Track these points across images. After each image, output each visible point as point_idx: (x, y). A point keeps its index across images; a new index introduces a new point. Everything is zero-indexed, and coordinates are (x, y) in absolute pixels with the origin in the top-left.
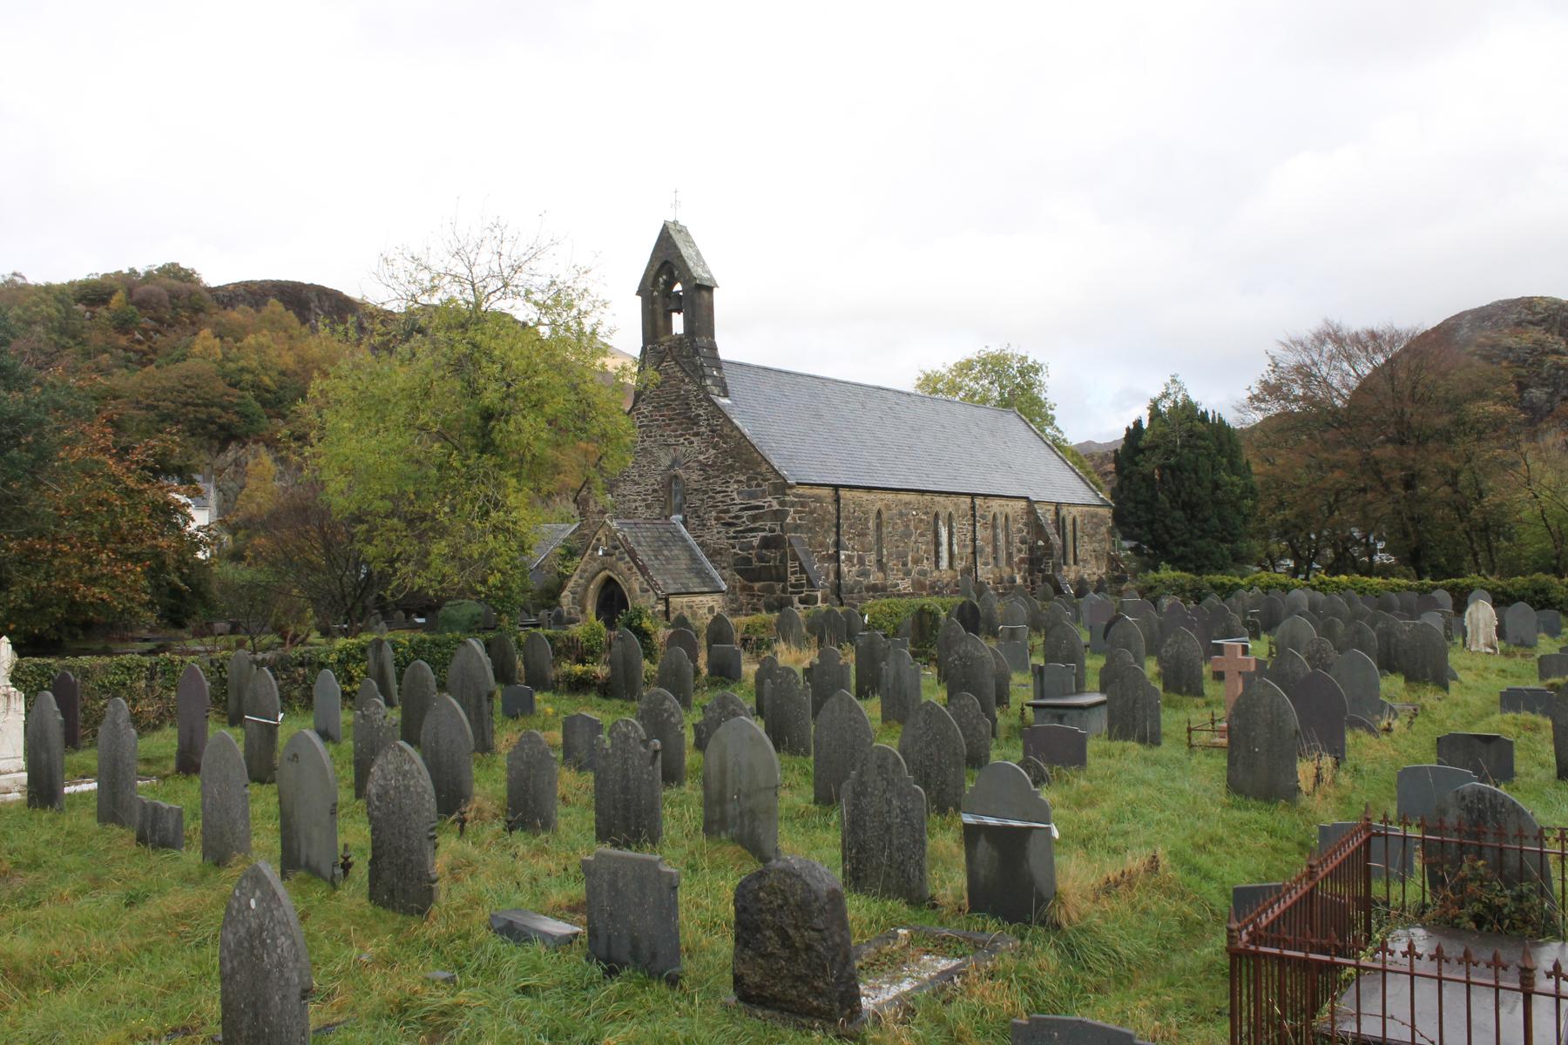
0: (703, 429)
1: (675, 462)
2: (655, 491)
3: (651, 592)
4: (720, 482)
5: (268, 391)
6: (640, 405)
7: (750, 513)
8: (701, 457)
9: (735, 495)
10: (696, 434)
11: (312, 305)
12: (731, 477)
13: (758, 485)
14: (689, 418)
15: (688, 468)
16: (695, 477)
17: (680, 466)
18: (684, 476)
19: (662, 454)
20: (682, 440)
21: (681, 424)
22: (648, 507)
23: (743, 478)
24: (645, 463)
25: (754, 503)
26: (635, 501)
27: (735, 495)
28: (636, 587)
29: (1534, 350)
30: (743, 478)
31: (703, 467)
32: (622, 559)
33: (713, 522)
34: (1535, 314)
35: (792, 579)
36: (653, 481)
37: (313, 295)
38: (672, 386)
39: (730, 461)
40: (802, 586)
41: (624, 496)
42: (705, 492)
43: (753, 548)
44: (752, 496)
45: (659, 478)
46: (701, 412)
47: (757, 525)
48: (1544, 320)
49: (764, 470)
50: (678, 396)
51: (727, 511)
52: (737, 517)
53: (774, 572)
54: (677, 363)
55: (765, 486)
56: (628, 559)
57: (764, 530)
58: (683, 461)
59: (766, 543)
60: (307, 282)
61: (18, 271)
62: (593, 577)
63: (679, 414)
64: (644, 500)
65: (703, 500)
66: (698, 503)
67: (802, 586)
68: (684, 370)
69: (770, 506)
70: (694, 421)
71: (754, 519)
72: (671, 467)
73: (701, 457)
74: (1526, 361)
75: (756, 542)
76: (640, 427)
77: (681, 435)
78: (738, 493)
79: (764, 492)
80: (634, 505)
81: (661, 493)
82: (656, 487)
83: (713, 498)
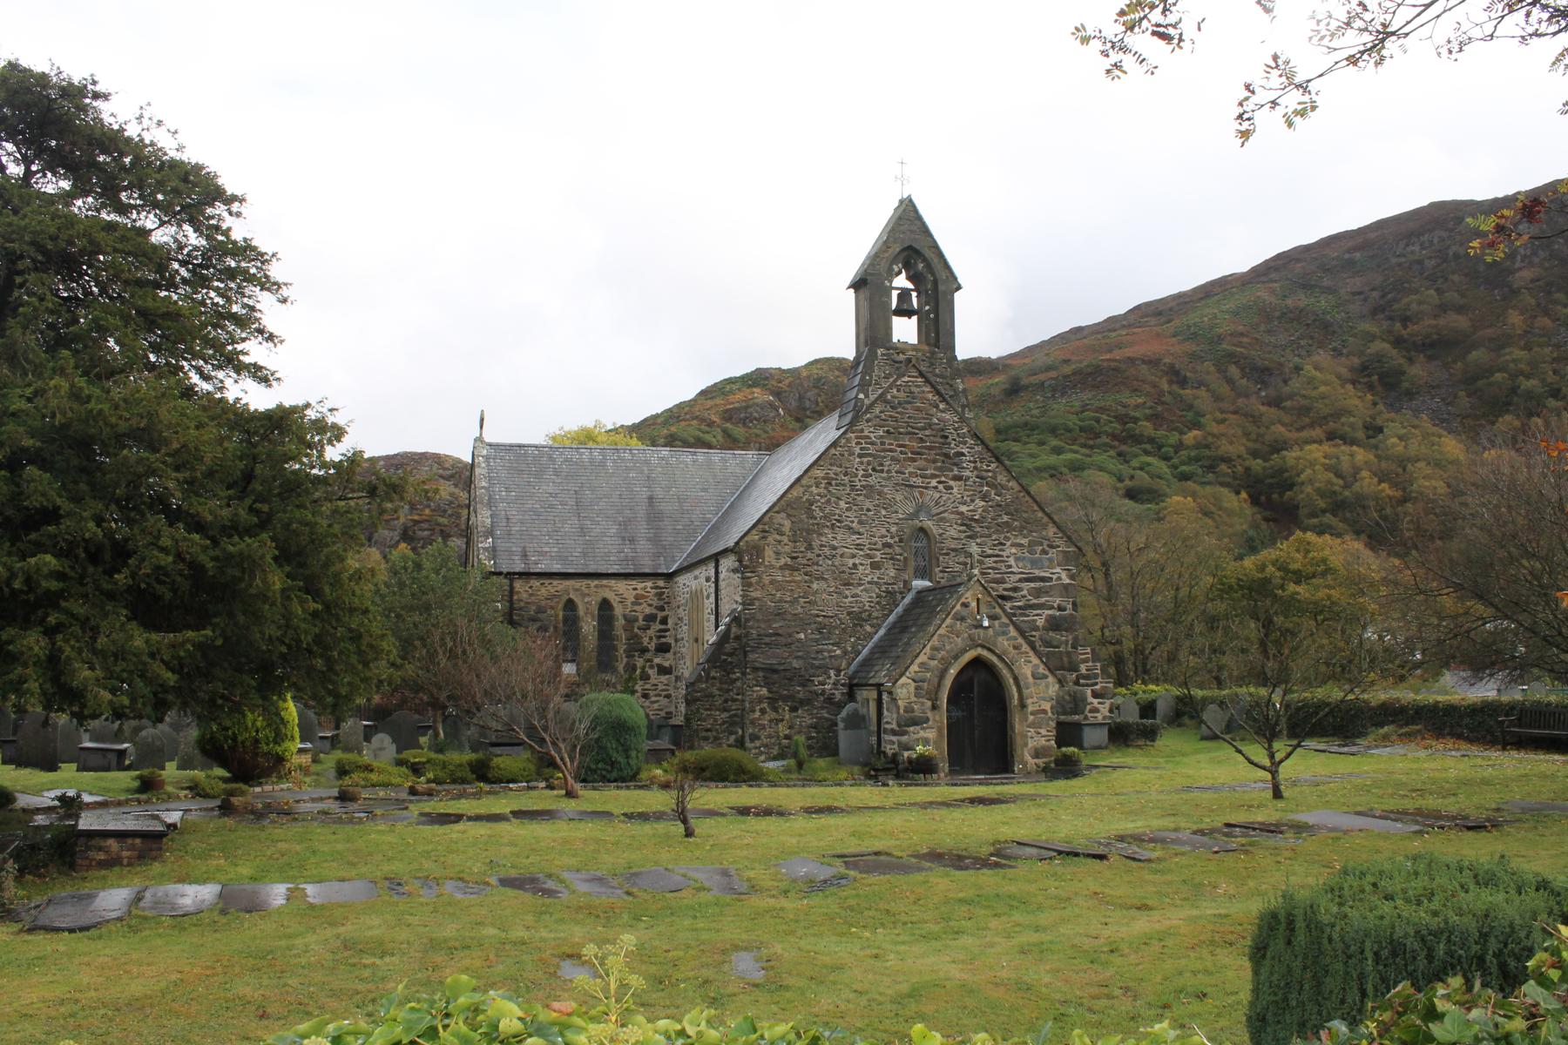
0: (967, 473)
1: (920, 508)
2: (887, 545)
6: (862, 425)
7: (1032, 585)
8: (964, 509)
9: (1012, 561)
10: (957, 478)
12: (1007, 539)
13: (1044, 552)
14: (947, 456)
15: (942, 519)
16: (953, 533)
17: (931, 516)
18: (935, 531)
19: (899, 497)
20: (934, 483)
21: (935, 461)
22: (875, 566)
23: (1024, 541)
24: (868, 504)
25: (1037, 573)
26: (854, 556)
27: (1012, 561)
29: (451, 502)
30: (1024, 541)
31: (967, 522)
34: (445, 469)
35: (1083, 669)
36: (883, 531)
38: (918, 409)
39: (1006, 518)
40: (1096, 676)
41: (835, 548)
43: (1036, 629)
44: (1034, 563)
45: (894, 529)
46: (965, 451)
47: (1042, 600)
48: (452, 476)
49: (1051, 534)
50: (930, 426)
51: (1002, 581)
52: (1015, 589)
53: (1065, 659)
54: (927, 381)
55: (1052, 553)
56: (1013, 632)
57: (1052, 608)
58: (934, 511)
59: (1054, 625)
62: (956, 658)
63: (930, 448)
64: (868, 556)
66: (958, 568)
67: (1096, 676)
68: (938, 393)
70: (953, 460)
71: (1038, 593)
72: (915, 515)
73: (964, 509)
74: (445, 511)
75: (1040, 622)
76: (860, 456)
77: (933, 476)
78: (1017, 559)
79: (1051, 560)
80: (851, 562)
81: (898, 550)
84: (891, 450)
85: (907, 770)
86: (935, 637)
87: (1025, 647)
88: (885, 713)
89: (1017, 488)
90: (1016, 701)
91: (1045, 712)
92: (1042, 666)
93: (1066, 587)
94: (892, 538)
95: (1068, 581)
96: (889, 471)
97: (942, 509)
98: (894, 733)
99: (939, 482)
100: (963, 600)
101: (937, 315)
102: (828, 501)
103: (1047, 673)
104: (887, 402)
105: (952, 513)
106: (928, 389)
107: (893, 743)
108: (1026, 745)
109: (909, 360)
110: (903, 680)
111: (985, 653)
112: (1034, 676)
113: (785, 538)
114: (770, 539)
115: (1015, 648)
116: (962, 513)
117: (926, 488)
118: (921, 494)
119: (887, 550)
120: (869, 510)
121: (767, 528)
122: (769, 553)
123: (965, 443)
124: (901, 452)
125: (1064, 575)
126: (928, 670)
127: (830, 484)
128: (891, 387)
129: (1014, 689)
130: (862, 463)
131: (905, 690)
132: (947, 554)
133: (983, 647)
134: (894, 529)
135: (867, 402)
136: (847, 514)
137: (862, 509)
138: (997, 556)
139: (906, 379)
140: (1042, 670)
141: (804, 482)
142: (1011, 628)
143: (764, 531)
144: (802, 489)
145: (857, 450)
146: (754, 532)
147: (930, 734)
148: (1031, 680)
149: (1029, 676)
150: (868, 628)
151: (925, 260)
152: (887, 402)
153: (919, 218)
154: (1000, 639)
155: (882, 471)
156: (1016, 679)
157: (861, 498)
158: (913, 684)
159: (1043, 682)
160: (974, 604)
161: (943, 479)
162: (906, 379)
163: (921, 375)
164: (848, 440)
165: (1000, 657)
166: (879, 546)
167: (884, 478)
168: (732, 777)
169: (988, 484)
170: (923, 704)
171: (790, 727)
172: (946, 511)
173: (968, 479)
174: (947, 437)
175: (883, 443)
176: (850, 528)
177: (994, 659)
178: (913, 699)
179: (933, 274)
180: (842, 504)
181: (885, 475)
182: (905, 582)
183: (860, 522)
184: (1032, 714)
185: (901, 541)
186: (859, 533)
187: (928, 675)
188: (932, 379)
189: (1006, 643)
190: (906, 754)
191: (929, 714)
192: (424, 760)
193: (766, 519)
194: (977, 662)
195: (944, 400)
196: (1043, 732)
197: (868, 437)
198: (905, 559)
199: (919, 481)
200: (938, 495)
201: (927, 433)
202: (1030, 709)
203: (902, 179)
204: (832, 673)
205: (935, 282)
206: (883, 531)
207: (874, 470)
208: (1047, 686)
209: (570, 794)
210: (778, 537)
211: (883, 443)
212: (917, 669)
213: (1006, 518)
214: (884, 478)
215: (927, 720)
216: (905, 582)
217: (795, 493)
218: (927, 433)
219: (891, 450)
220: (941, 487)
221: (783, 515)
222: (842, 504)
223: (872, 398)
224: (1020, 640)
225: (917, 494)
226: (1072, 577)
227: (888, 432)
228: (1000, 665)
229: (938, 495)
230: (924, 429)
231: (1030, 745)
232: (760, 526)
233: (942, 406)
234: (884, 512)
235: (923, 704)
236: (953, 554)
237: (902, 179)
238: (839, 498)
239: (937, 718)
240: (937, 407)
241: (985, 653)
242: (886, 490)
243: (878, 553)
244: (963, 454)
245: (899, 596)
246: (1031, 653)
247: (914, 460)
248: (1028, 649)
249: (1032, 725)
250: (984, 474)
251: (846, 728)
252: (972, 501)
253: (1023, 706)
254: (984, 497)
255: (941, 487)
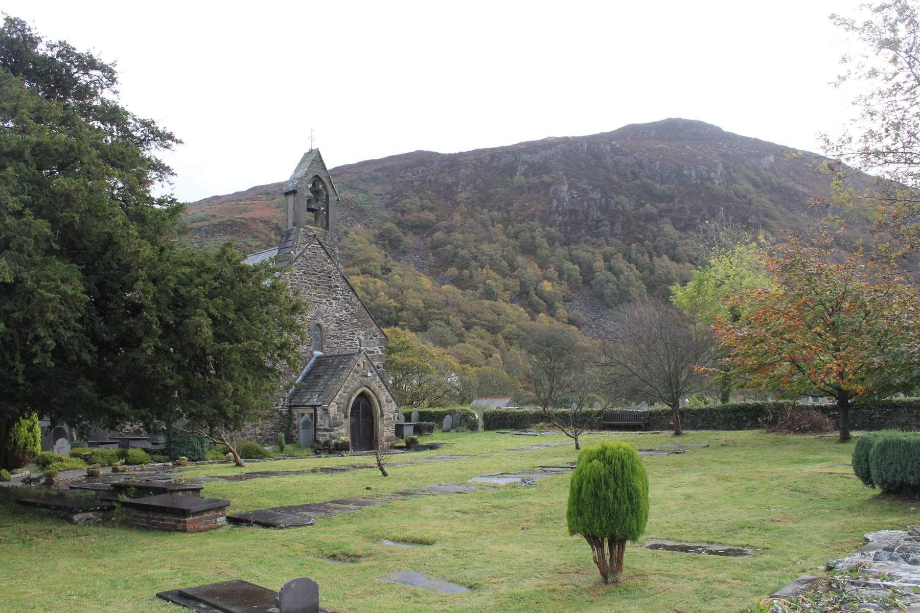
0: (339, 296)
10: (335, 299)
13: (371, 338)
14: (330, 287)
15: (328, 320)
16: (332, 327)
18: (325, 326)
20: (324, 301)
31: (339, 322)
38: (318, 262)
46: (339, 285)
54: (323, 247)
55: (375, 339)
58: (324, 316)
62: (355, 391)
63: (323, 282)
65: (338, 343)
66: (335, 345)
68: (327, 254)
69: (377, 352)
73: (337, 315)
77: (324, 297)
79: (374, 342)
83: (345, 343)
84: (306, 283)
85: (334, 449)
87: (383, 387)
88: (319, 420)
89: (361, 305)
90: (379, 414)
91: (390, 419)
93: (380, 356)
95: (381, 353)
96: (304, 293)
98: (326, 430)
101: (328, 213)
104: (304, 257)
106: (323, 251)
107: (326, 436)
109: (315, 236)
110: (333, 403)
111: (367, 389)
112: (387, 402)
116: (336, 317)
118: (319, 306)
123: (338, 281)
125: (379, 350)
126: (343, 398)
128: (306, 249)
129: (378, 407)
133: (366, 386)
135: (295, 256)
139: (313, 245)
140: (390, 398)
147: (344, 431)
150: (294, 376)
151: (323, 183)
152: (304, 257)
153: (322, 161)
156: (379, 402)
160: (362, 365)
162: (313, 245)
163: (320, 244)
164: (286, 276)
165: (373, 392)
168: (254, 456)
169: (348, 303)
170: (341, 415)
171: (262, 429)
173: (340, 299)
174: (330, 277)
175: (302, 278)
177: (370, 392)
178: (337, 413)
179: (327, 191)
182: (311, 352)
185: (309, 330)
188: (325, 246)
190: (334, 441)
191: (343, 421)
192: (90, 453)
194: (363, 395)
195: (330, 258)
196: (390, 428)
197: (295, 275)
200: (326, 307)
201: (322, 274)
203: (312, 138)
204: (281, 399)
205: (327, 196)
209: (239, 465)
211: (302, 278)
213: (355, 320)
216: (311, 352)
218: (322, 274)
219: (306, 283)
223: (298, 254)
225: (317, 306)
226: (383, 351)
227: (304, 272)
228: (373, 395)
229: (326, 307)
230: (320, 272)
233: (329, 261)
237: (312, 138)
240: (326, 261)
241: (367, 389)
244: (337, 287)
245: (308, 360)
246: (386, 390)
247: (316, 288)
250: (346, 297)
251: (303, 428)
253: (382, 415)
254: (346, 309)
255: (327, 303)
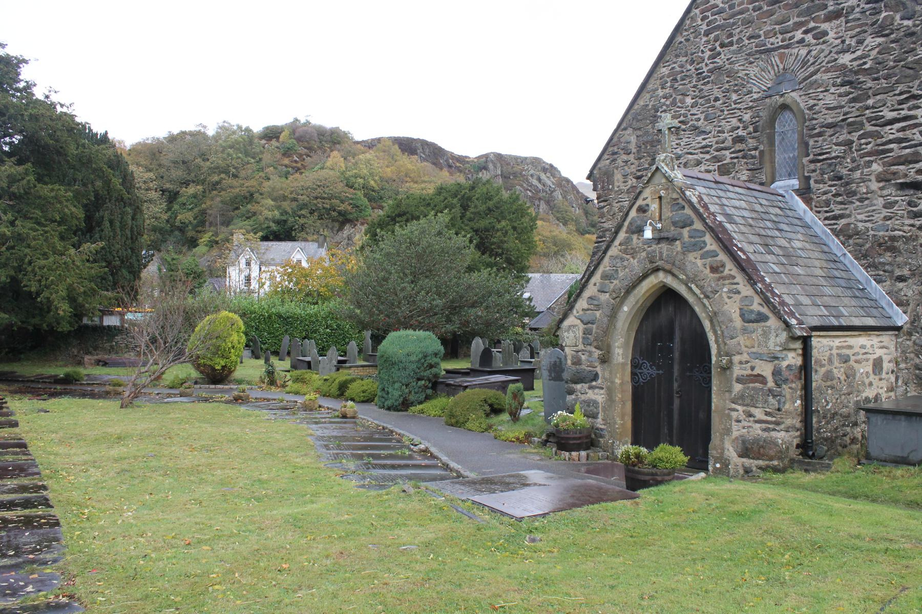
1: (780, 79)
2: (739, 140)
3: (773, 322)
4: (891, 100)
5: (373, 191)
8: (845, 59)
11: (418, 151)
19: (753, 71)
20: (799, 35)
24: (717, 93)
28: (732, 308)
32: (698, 246)
33: (875, 186)
36: (734, 122)
37: (419, 145)
42: (853, 127)
45: (747, 117)
56: (711, 244)
58: (801, 76)
60: (415, 137)
61: (226, 120)
62: (629, 290)
64: (716, 159)
65: (849, 143)
66: (837, 151)
73: (845, 59)
76: (707, 34)
77: (798, 25)
81: (752, 143)
82: (740, 132)
83: (878, 135)
84: (741, 13)
86: (606, 260)
87: (730, 268)
92: (757, 300)
94: (745, 128)
96: (740, 40)
97: (812, 69)
99: (806, 32)
100: (640, 202)
102: (674, 103)
103: (765, 310)
105: (827, 71)
108: (728, 431)
113: (631, 158)
114: (620, 162)
115: (714, 269)
116: (844, 66)
117: (787, 47)
118: (782, 57)
119: (738, 146)
120: (717, 99)
121: (615, 149)
122: (618, 176)
124: (754, 10)
126: (598, 307)
127: (675, 80)
130: (708, 42)
131: (571, 334)
132: (820, 134)
134: (747, 117)
136: (694, 111)
137: (708, 101)
138: (906, 118)
141: (650, 86)
142: (708, 238)
143: (614, 153)
144: (648, 96)
145: (704, 27)
146: (606, 156)
148: (738, 323)
149: (736, 316)
154: (691, 256)
155: (731, 44)
157: (709, 86)
158: (582, 326)
159: (759, 327)
161: (812, 24)
166: (728, 143)
167: (734, 52)
172: (818, 70)
176: (696, 128)
178: (581, 347)
180: (689, 101)
181: (735, 47)
183: (706, 119)
184: (739, 380)
185: (755, 131)
186: (704, 132)
187: (598, 314)
189: (699, 262)
191: (599, 369)
193: (615, 139)
196: (759, 413)
198: (762, 153)
199: (777, 41)
200: (804, 52)
202: (737, 371)
206: (734, 122)
207: (722, 45)
208: (766, 334)
210: (625, 157)
212: (586, 306)
214: (734, 52)
215: (595, 377)
217: (641, 102)
219: (741, 13)
220: (809, 38)
221: (630, 131)
222: (689, 101)
224: (722, 257)
225: (776, 59)
229: (804, 52)
231: (735, 434)
232: (610, 149)
234: (734, 97)
235: (590, 353)
236: (831, 131)
238: (684, 95)
239: (607, 375)
242: (736, 67)
243: (727, 153)
246: (740, 278)
248: (735, 272)
249: (739, 399)
252: (860, 42)
254: (881, 31)
255: (809, 38)
